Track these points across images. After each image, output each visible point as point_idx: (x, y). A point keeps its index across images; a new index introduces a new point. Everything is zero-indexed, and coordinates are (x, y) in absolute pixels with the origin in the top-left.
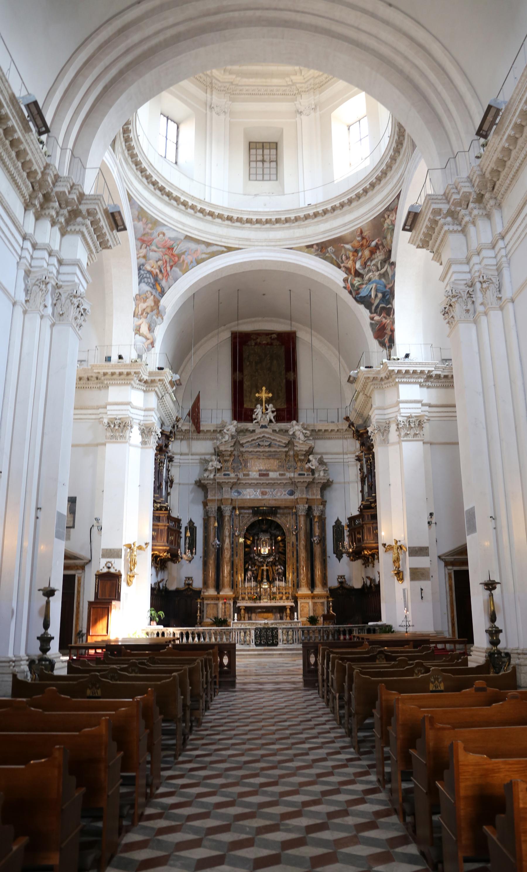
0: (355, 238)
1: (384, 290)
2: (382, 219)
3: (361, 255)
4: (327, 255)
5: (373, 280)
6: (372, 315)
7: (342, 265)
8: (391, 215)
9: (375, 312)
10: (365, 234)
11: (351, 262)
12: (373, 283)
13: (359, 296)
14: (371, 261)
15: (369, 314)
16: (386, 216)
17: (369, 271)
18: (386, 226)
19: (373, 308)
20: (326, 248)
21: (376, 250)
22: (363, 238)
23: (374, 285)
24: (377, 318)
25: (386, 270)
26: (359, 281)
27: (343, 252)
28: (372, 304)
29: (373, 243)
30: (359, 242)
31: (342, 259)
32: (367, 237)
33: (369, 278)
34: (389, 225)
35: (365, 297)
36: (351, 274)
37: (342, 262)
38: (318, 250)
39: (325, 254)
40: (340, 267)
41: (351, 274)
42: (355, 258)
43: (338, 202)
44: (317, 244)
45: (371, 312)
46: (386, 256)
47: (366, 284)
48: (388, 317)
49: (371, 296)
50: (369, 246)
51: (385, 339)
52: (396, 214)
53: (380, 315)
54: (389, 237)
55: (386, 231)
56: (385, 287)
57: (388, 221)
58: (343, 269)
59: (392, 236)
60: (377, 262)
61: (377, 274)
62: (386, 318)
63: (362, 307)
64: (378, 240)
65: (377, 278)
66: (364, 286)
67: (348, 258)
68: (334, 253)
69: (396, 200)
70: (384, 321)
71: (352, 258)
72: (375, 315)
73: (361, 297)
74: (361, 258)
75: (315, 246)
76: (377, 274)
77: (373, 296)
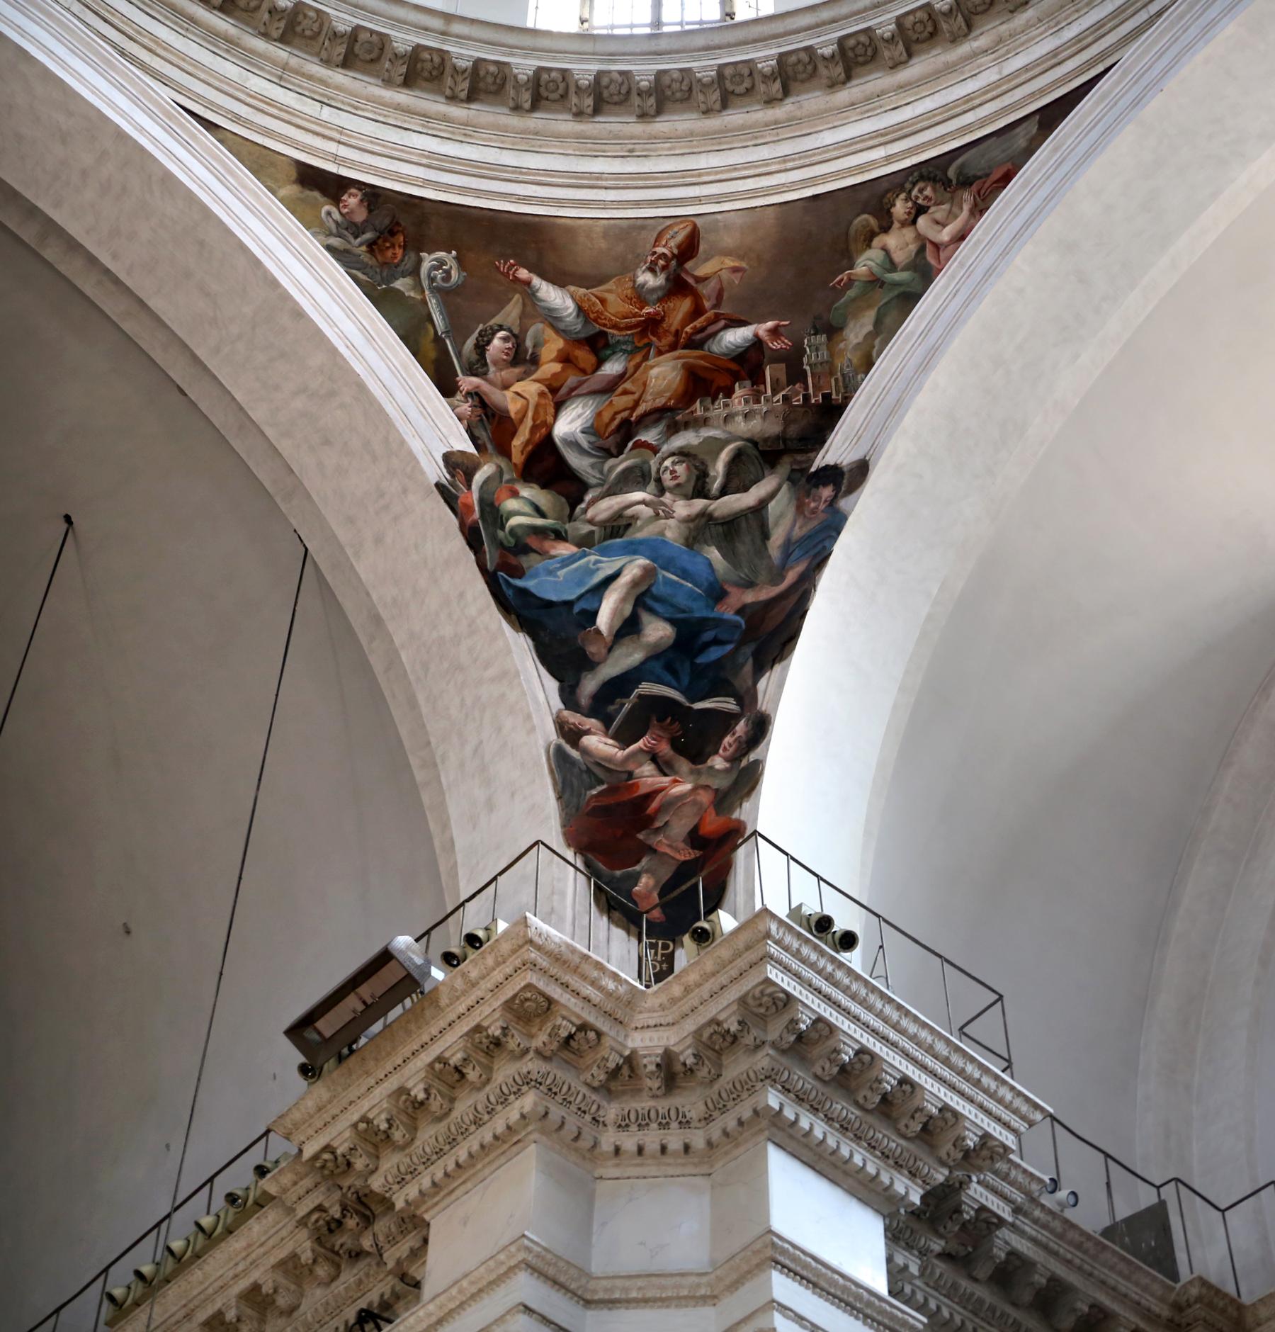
0: (627, 269)
1: (700, 610)
2: (867, 219)
3: (621, 377)
4: (401, 284)
5: (641, 533)
6: (574, 718)
7: (467, 382)
8: (939, 212)
9: (601, 706)
10: (702, 268)
11: (530, 388)
12: (633, 549)
13: (518, 583)
14: (674, 429)
15: (557, 704)
16: (900, 208)
17: (636, 478)
18: (866, 263)
19: (590, 685)
20: (418, 244)
21: (736, 377)
22: (678, 286)
23: (634, 567)
24: (599, 743)
25: (762, 504)
26: (540, 513)
27: (511, 313)
28: (587, 664)
29: (735, 337)
30: (639, 296)
31: (481, 348)
32: (706, 290)
33: (619, 515)
34: (891, 265)
35: (550, 604)
36: (504, 451)
37: (478, 366)
38: (357, 230)
39: (391, 270)
40: (447, 388)
41: (504, 451)
42: (572, 380)
43: (595, 67)
44: (373, 195)
45: (569, 696)
46: (793, 430)
47: (585, 542)
48: (684, 765)
49: (594, 615)
50: (692, 344)
51: (636, 878)
52: (979, 210)
53: (624, 737)
54: (856, 332)
55: (851, 293)
56: (717, 593)
57: (898, 242)
58: (466, 408)
59: (884, 331)
60: (716, 446)
61: (683, 508)
62: (663, 767)
63: (520, 647)
64: (774, 332)
65: (672, 531)
66: (564, 550)
67: (523, 359)
68: (446, 295)
69: (1032, 126)
70: (647, 776)
71: (550, 368)
72: (592, 723)
73: (524, 592)
74: (611, 387)
75: (352, 200)
76: (683, 508)
77: (604, 620)
